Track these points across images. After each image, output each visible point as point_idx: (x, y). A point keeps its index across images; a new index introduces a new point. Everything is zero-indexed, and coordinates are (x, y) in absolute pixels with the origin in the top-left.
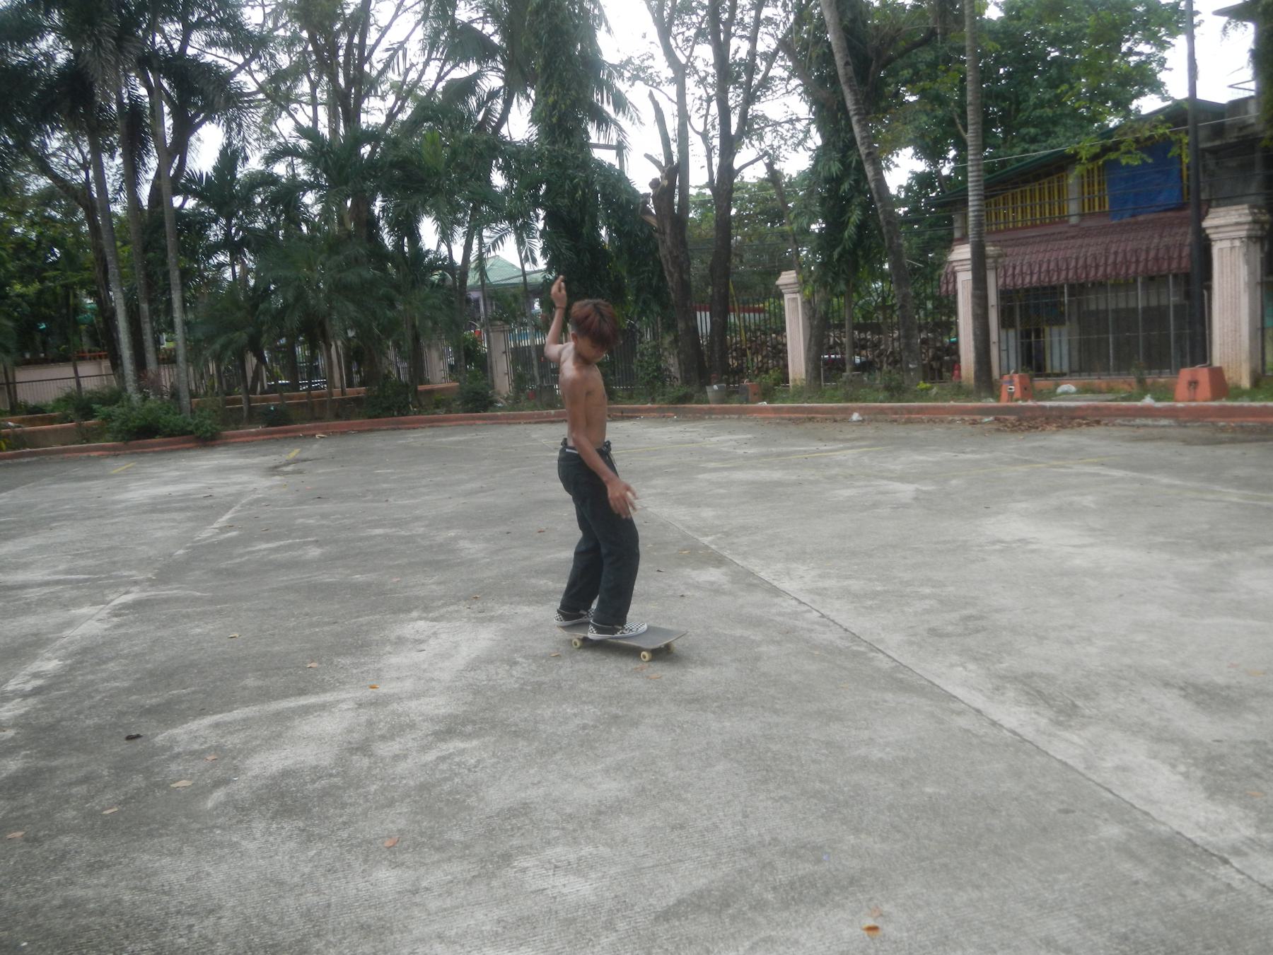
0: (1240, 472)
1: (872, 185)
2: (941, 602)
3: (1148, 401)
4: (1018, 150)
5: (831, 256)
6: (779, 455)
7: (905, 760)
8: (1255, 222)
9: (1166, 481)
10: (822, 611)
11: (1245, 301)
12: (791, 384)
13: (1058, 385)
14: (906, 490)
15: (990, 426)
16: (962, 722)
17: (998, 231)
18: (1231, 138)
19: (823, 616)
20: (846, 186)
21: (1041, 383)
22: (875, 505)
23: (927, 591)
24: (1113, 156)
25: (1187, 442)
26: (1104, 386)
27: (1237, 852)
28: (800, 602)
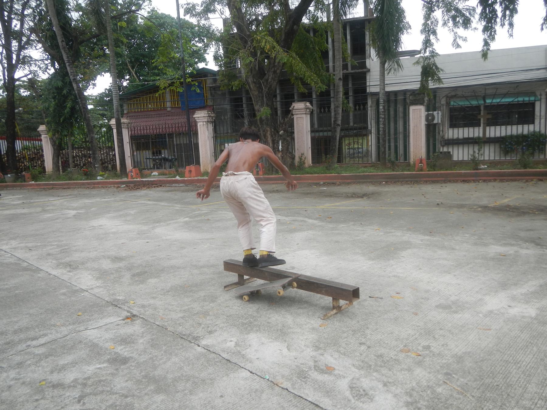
0: (187, 200)
1: (76, 92)
2: (58, 246)
3: (178, 178)
4: (152, 78)
5: (60, 120)
6: (31, 203)
7: (14, 287)
8: (209, 116)
9: (163, 204)
10: (13, 254)
11: (208, 143)
12: (47, 173)
13: (152, 172)
14: (73, 212)
15: (123, 189)
16: (39, 275)
17: (141, 111)
18: (218, 83)
19: (12, 255)
20: (65, 92)
21: (146, 172)
22: (57, 219)
23: (56, 243)
24: (172, 88)
25: (183, 191)
26: (167, 172)
27: (92, 289)
28: (6, 252)
